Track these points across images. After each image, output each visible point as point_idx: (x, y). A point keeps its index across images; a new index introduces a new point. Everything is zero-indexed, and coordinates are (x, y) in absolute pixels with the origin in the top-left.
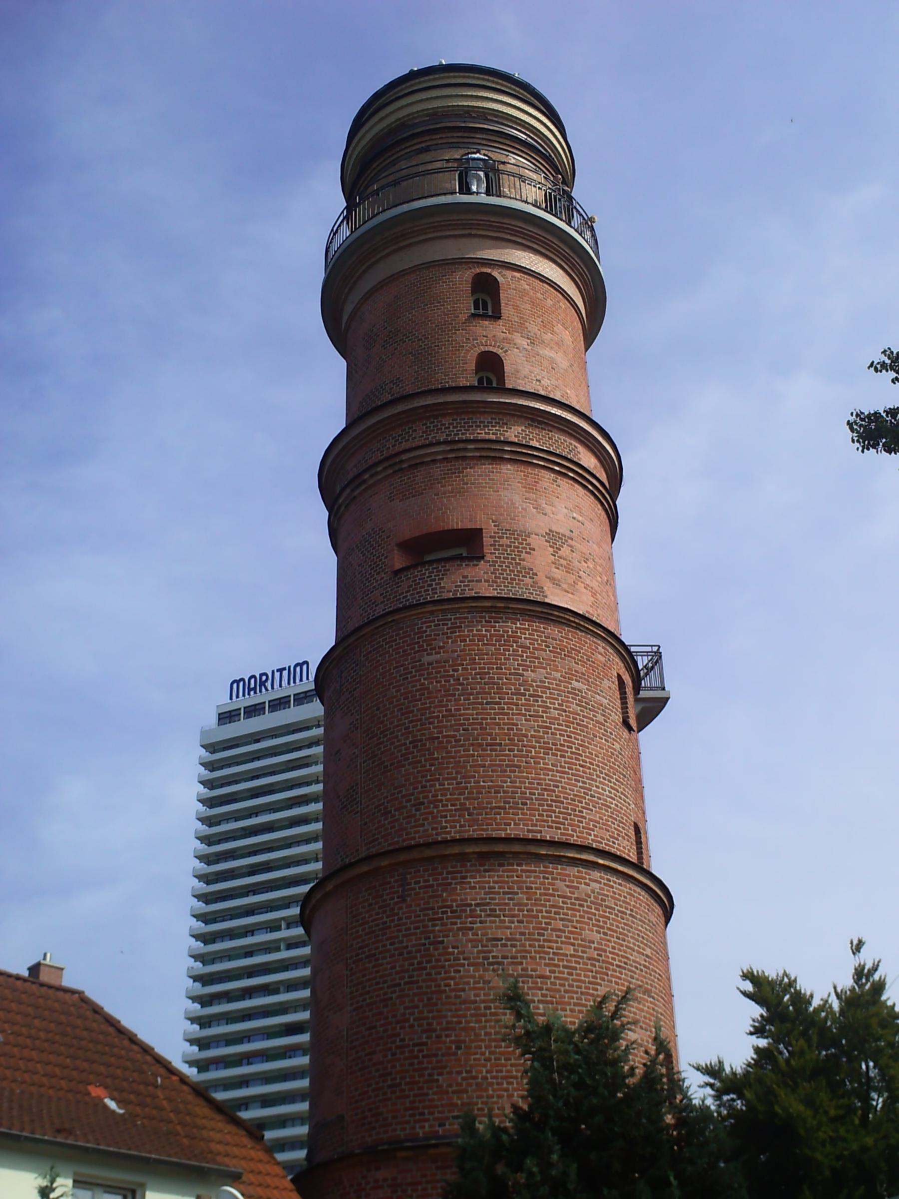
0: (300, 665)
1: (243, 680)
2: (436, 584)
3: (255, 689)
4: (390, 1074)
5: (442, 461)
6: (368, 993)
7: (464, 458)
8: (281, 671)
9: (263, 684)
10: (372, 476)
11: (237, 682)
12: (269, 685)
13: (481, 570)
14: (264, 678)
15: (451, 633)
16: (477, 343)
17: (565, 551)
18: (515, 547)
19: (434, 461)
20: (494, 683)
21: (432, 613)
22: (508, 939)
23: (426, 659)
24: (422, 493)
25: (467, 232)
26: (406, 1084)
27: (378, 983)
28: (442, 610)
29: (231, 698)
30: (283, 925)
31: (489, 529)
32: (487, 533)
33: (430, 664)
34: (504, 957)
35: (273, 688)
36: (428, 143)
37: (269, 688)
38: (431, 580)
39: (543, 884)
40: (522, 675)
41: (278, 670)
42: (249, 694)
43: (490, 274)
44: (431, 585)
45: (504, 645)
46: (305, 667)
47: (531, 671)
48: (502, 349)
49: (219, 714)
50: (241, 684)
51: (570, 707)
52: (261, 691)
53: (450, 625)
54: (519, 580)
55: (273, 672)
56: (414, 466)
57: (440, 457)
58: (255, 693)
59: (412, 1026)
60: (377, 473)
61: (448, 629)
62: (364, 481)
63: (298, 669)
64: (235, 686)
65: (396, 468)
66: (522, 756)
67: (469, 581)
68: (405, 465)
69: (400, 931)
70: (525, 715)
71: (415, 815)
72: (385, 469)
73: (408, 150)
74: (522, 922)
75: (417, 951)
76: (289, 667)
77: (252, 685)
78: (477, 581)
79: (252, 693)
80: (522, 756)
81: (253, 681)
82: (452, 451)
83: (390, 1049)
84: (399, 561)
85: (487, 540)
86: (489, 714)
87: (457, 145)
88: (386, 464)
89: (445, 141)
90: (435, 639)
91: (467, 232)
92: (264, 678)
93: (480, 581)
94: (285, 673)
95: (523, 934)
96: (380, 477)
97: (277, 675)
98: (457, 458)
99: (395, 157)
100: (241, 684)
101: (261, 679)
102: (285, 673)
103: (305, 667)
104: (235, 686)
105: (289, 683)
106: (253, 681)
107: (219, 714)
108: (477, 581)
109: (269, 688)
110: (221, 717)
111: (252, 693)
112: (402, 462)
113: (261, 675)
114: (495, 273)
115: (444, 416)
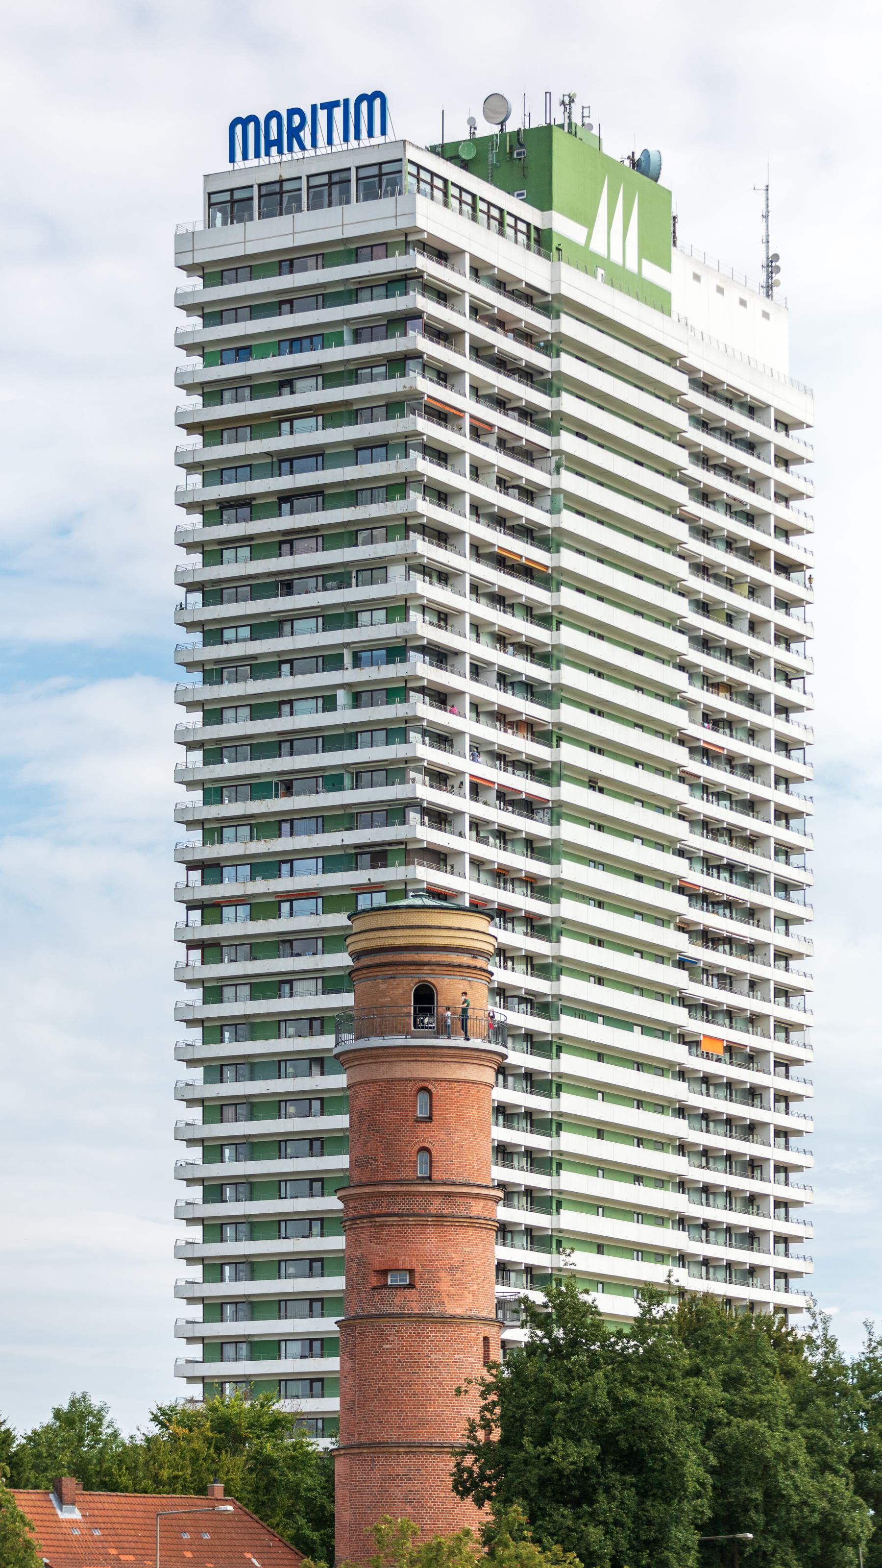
0: (370, 99)
1: (253, 118)
3: (278, 143)
7: (407, 1225)
8: (329, 106)
9: (294, 133)
11: (243, 122)
12: (306, 135)
13: (412, 1294)
14: (297, 120)
17: (458, 1275)
23: (386, 1346)
29: (232, 159)
30: (348, 660)
31: (419, 1269)
35: (314, 145)
37: (308, 143)
41: (324, 106)
42: (268, 154)
46: (377, 103)
49: (210, 194)
50: (251, 126)
52: (290, 149)
55: (314, 107)
56: (383, 1226)
58: (280, 152)
63: (364, 106)
64: (239, 129)
76: (346, 101)
77: (274, 136)
79: (274, 150)
81: (274, 122)
84: (375, 1281)
85: (417, 1275)
92: (297, 120)
94: (338, 113)
97: (322, 115)
100: (251, 126)
101: (290, 121)
102: (338, 113)
103: (377, 103)
104: (239, 129)
105: (346, 139)
106: (274, 122)
107: (210, 194)
109: (308, 143)
110: (215, 199)
111: (274, 150)
113: (291, 112)
114: (430, 1087)
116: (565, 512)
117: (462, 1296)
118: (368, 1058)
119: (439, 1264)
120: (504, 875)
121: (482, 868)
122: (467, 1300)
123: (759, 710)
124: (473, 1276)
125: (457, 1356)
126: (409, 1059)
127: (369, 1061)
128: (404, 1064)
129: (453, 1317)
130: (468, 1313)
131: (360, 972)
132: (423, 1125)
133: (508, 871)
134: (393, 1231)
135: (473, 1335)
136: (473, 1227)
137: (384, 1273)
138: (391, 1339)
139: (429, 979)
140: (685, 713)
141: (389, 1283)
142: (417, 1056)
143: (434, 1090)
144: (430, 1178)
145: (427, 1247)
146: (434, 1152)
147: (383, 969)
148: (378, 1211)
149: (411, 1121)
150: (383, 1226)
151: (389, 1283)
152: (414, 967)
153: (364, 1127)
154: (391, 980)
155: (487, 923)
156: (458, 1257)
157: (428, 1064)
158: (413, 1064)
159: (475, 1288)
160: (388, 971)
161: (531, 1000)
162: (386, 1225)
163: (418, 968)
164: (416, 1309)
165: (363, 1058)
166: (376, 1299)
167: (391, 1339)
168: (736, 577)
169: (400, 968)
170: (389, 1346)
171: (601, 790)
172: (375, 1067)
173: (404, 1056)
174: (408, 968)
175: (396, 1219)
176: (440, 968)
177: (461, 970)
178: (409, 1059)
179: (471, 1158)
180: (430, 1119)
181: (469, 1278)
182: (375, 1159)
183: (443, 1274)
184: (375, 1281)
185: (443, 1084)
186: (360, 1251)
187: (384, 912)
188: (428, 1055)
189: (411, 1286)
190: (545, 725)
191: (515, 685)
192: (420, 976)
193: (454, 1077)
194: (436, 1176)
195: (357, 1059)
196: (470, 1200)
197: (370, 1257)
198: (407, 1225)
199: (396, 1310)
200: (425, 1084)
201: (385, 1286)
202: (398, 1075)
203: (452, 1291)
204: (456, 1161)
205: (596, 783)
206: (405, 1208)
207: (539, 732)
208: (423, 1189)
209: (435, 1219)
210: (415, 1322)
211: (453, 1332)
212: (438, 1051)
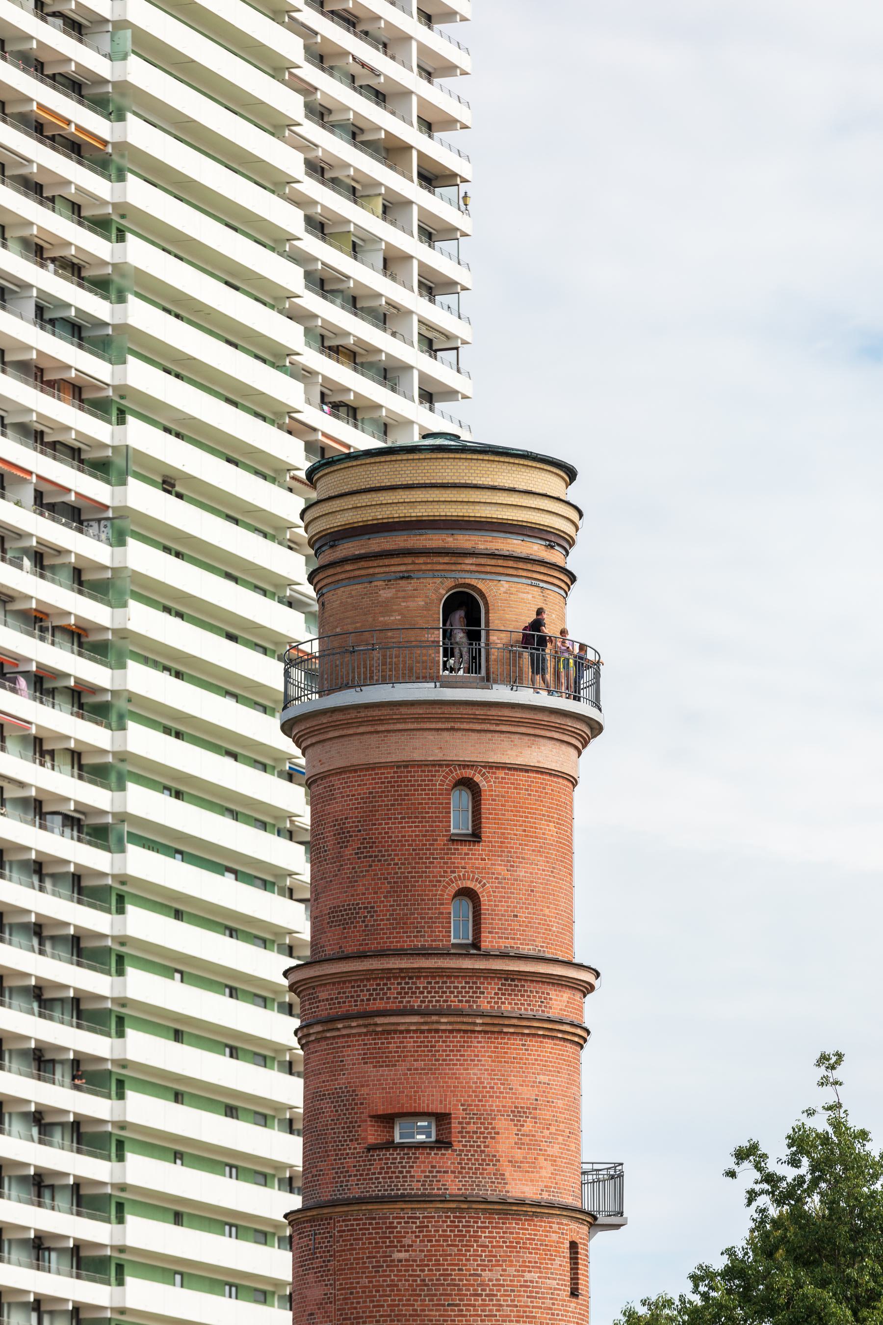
2: (407, 1172)
5: (415, 1031)
7: (437, 1031)
10: (344, 1027)
13: (447, 1159)
15: (420, 1232)
16: (455, 877)
17: (528, 1126)
18: (481, 1133)
19: (408, 1031)
20: (455, 1285)
21: (403, 1209)
23: (397, 1256)
24: (395, 1065)
25: (448, 725)
28: (412, 1209)
31: (458, 1113)
32: (456, 1118)
36: (410, 567)
38: (402, 1167)
40: (480, 1275)
44: (401, 1172)
45: (466, 1246)
47: (489, 1270)
48: (480, 883)
51: (520, 1301)
53: (418, 1224)
54: (483, 1169)
56: (389, 1032)
57: (413, 1028)
60: (351, 1027)
61: (416, 1227)
62: (338, 1029)
65: (371, 1028)
67: (438, 1172)
68: (380, 1029)
70: (480, 1316)
72: (358, 1026)
73: (387, 569)
78: (444, 1172)
82: (426, 1023)
84: (372, 1135)
85: (455, 1124)
86: (450, 1316)
87: (443, 574)
88: (361, 1022)
89: (429, 567)
90: (405, 1237)
91: (448, 725)
93: (446, 1172)
96: (354, 1031)
98: (429, 1031)
99: (371, 571)
108: (444, 1172)
112: (376, 1025)
114: (478, 778)
115: (418, 978)
116: (133, 59)
117: (534, 1163)
118: (361, 724)
119: (496, 1104)
120: (41, 620)
121: (11, 607)
122: (544, 1173)
123: (393, 390)
124: (553, 1129)
125: (528, 1276)
126: (440, 726)
127: (362, 730)
128: (430, 736)
129: (522, 1203)
130: (545, 1196)
131: (339, 569)
132: (465, 849)
133: (47, 615)
134: (410, 1043)
135: (555, 1237)
136: (553, 1038)
137: (387, 1120)
138: (407, 1241)
139: (473, 582)
140: (300, 386)
141: (397, 1140)
142: (454, 720)
143: (483, 785)
144: (476, 945)
145: (474, 1073)
146: (484, 899)
147: (387, 562)
148: (380, 1005)
149: (442, 840)
150: (389, 1032)
151: (397, 1140)
152: (446, 559)
153: (348, 852)
154: (403, 583)
155: (563, 485)
156: (528, 1093)
157: (475, 736)
158: (446, 734)
159: (554, 1150)
160: (398, 566)
161: (79, 820)
162: (395, 1032)
163: (454, 560)
164: (453, 1186)
165: (348, 725)
166: (376, 1167)
167: (407, 1241)
168: (364, 186)
169: (421, 560)
170: (402, 1255)
171: (180, 496)
172: (373, 740)
173: (429, 719)
174: (435, 559)
175: (415, 1019)
176: (493, 562)
177: (529, 567)
178: (440, 726)
179: (547, 911)
180: (476, 836)
181: (546, 1132)
182: (371, 910)
183: (501, 1123)
184: (372, 1135)
185: (501, 774)
186: (342, 1080)
187: (388, 458)
188: (476, 719)
189: (443, 1143)
190: (102, 389)
191: (57, 323)
192: (457, 575)
193: (519, 761)
194: (488, 942)
195: (335, 727)
196: (548, 989)
197: (364, 1091)
198: (437, 1031)
199: (416, 1188)
200: (468, 773)
201: (390, 1145)
202: (417, 756)
203: (518, 1154)
204: (523, 916)
205: (173, 486)
206: (434, 1001)
207: (87, 399)
208: (467, 964)
209: (488, 1020)
210: (452, 1210)
211: (519, 1229)
212: (493, 712)
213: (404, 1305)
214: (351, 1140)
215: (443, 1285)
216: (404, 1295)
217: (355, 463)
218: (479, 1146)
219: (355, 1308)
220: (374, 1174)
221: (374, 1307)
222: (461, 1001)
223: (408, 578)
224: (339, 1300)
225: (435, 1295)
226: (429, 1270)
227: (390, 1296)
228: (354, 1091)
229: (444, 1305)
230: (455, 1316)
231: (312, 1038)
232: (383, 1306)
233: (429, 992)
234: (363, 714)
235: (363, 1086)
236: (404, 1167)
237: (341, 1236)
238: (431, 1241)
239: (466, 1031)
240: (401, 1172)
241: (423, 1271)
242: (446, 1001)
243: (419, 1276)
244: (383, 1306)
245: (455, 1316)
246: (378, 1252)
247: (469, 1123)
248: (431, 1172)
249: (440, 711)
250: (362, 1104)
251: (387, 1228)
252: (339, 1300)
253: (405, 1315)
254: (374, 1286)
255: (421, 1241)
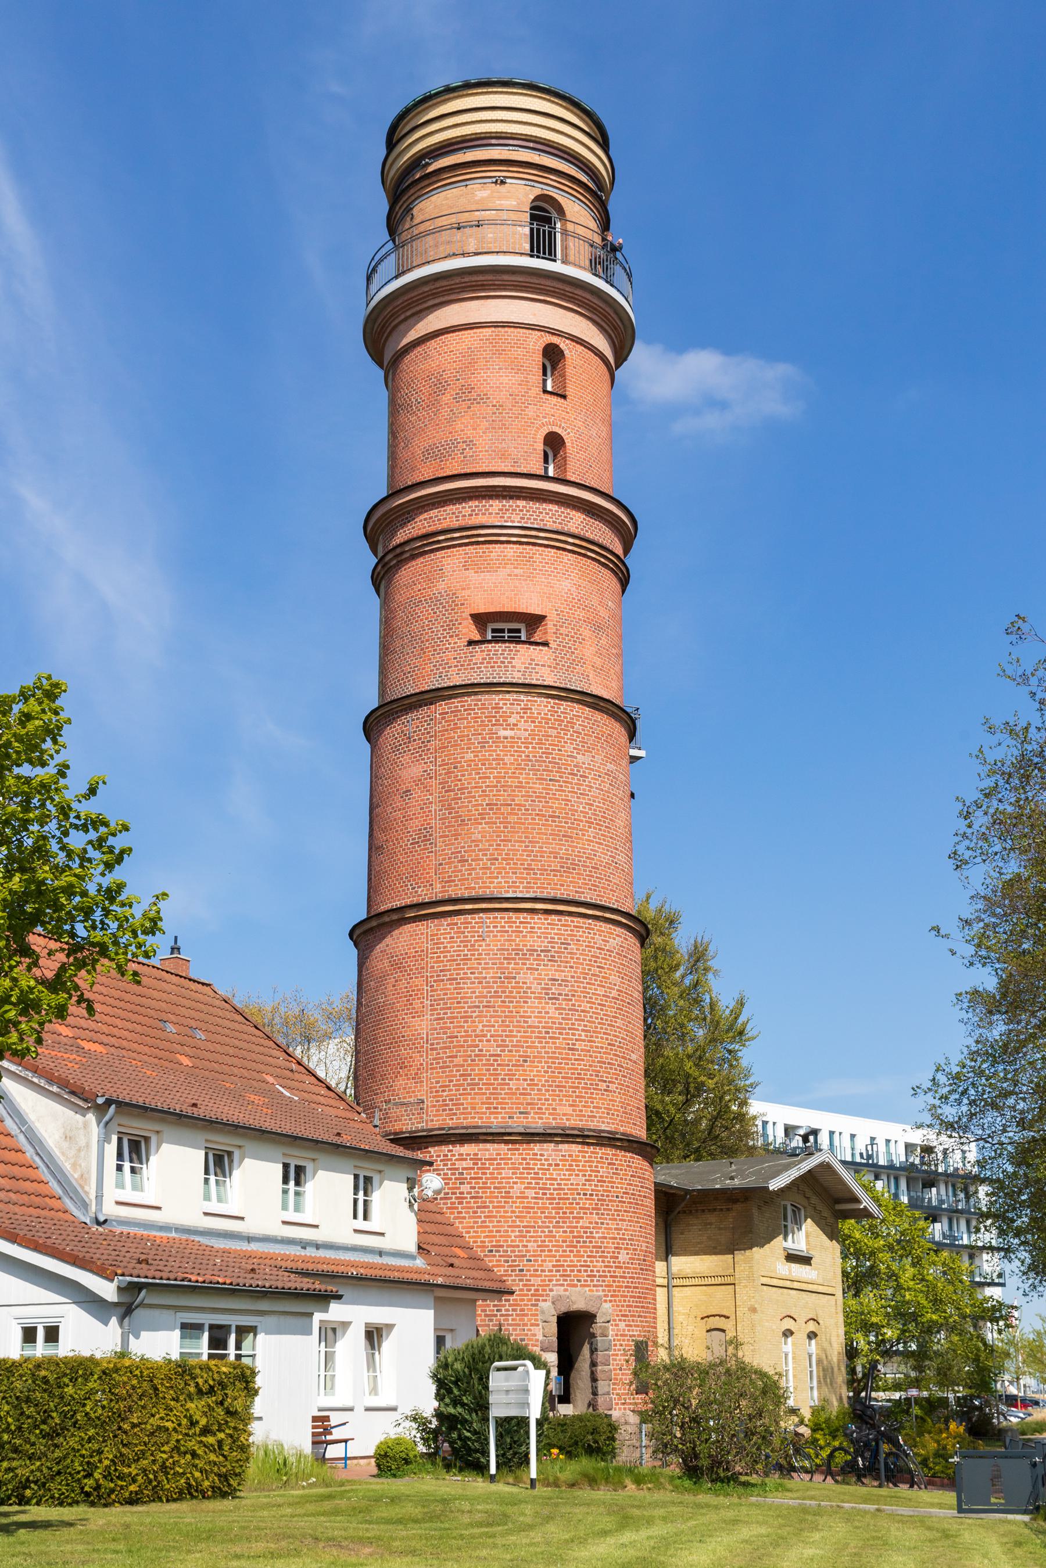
4: (470, 1075)
6: (450, 1008)
22: (562, 980)
23: (502, 733)
26: (483, 1084)
27: (458, 1003)
33: (506, 738)
34: (560, 994)
39: (587, 937)
43: (557, 346)
44: (503, 662)
59: (488, 1041)
66: (574, 828)
69: (480, 964)
71: (490, 868)
74: (571, 967)
75: (494, 982)
80: (574, 828)
83: (470, 1056)
93: (543, 665)
95: (573, 977)
114: (562, 346)
134: (510, 550)
138: (512, 720)
167: (512, 720)
170: (508, 733)
182: (470, 443)
185: (580, 348)
195: (435, 295)
197: (465, 593)
200: (555, 340)
213: (510, 777)
214: (451, 636)
215: (545, 762)
216: (510, 769)
217: (451, 95)
218: (570, 648)
219: (460, 780)
220: (476, 664)
221: (480, 778)
222: (554, 522)
223: (503, 183)
224: (440, 775)
225: (539, 770)
226: (533, 748)
227: (496, 769)
228: (454, 594)
229: (546, 780)
230: (557, 790)
231: (407, 555)
232: (489, 778)
233: (528, 511)
234: (466, 280)
235: (464, 589)
236: (506, 658)
237: (443, 718)
238: (533, 722)
239: (558, 548)
240: (503, 662)
241: (528, 748)
242: (542, 520)
243: (524, 752)
244: (489, 778)
245: (557, 790)
246: (484, 730)
247: (562, 626)
248: (530, 664)
249: (537, 282)
250: (462, 604)
251: (493, 708)
252: (440, 775)
253: (511, 786)
254: (479, 760)
255: (525, 722)
